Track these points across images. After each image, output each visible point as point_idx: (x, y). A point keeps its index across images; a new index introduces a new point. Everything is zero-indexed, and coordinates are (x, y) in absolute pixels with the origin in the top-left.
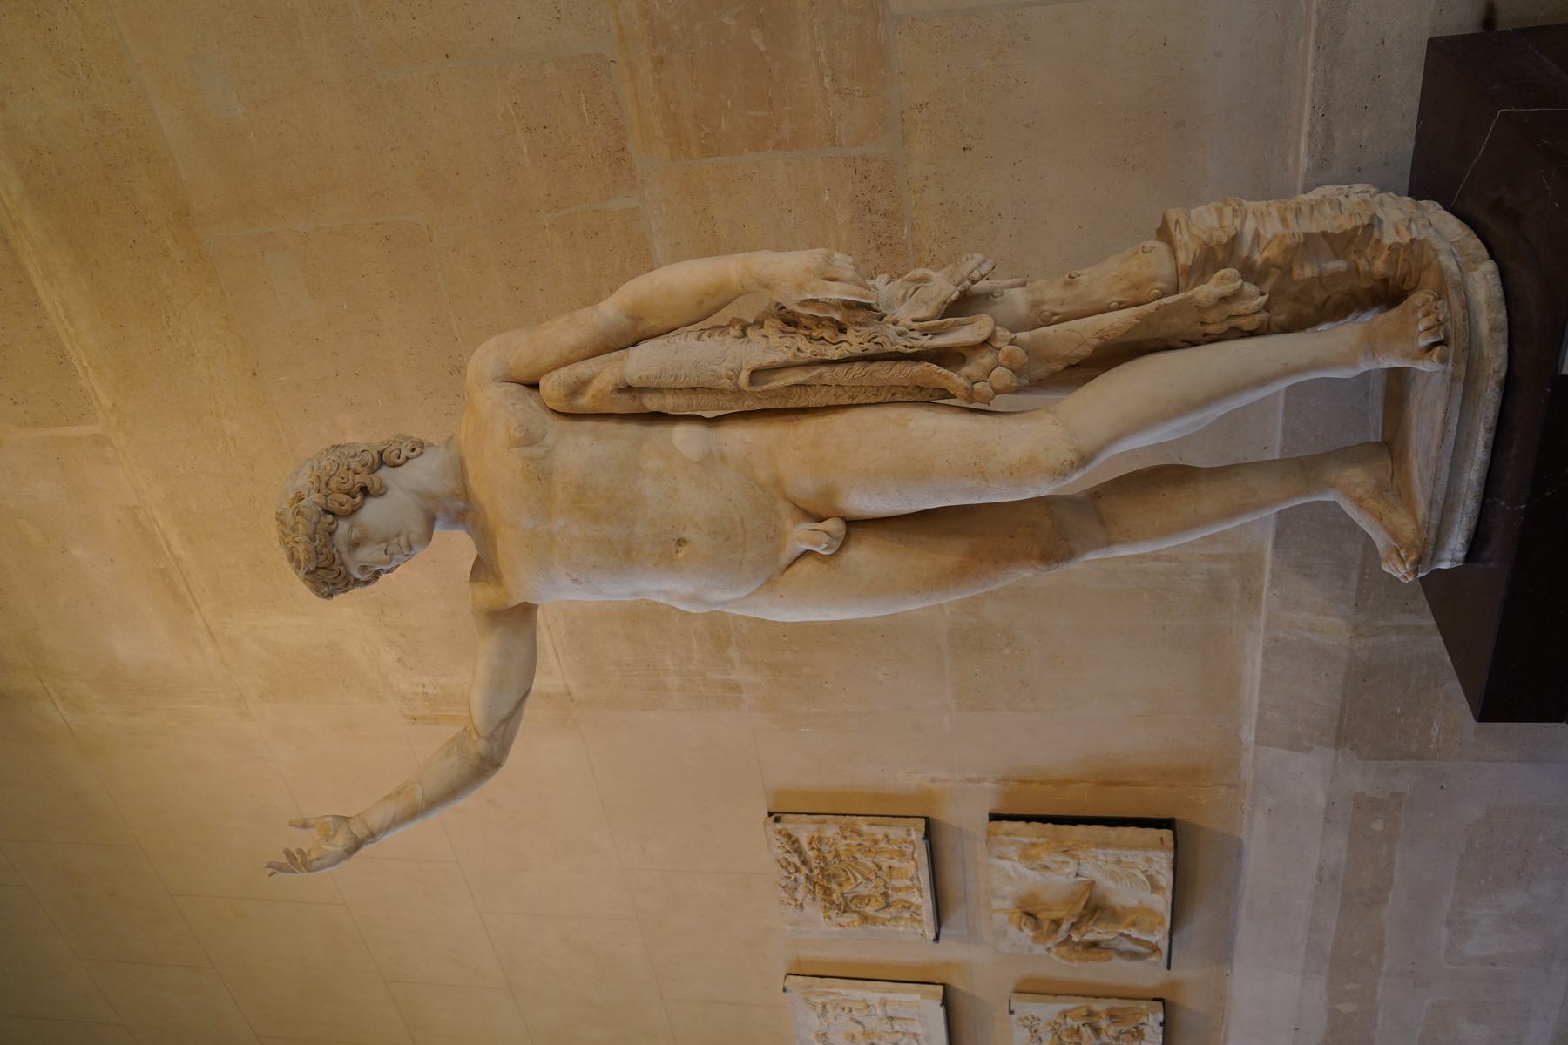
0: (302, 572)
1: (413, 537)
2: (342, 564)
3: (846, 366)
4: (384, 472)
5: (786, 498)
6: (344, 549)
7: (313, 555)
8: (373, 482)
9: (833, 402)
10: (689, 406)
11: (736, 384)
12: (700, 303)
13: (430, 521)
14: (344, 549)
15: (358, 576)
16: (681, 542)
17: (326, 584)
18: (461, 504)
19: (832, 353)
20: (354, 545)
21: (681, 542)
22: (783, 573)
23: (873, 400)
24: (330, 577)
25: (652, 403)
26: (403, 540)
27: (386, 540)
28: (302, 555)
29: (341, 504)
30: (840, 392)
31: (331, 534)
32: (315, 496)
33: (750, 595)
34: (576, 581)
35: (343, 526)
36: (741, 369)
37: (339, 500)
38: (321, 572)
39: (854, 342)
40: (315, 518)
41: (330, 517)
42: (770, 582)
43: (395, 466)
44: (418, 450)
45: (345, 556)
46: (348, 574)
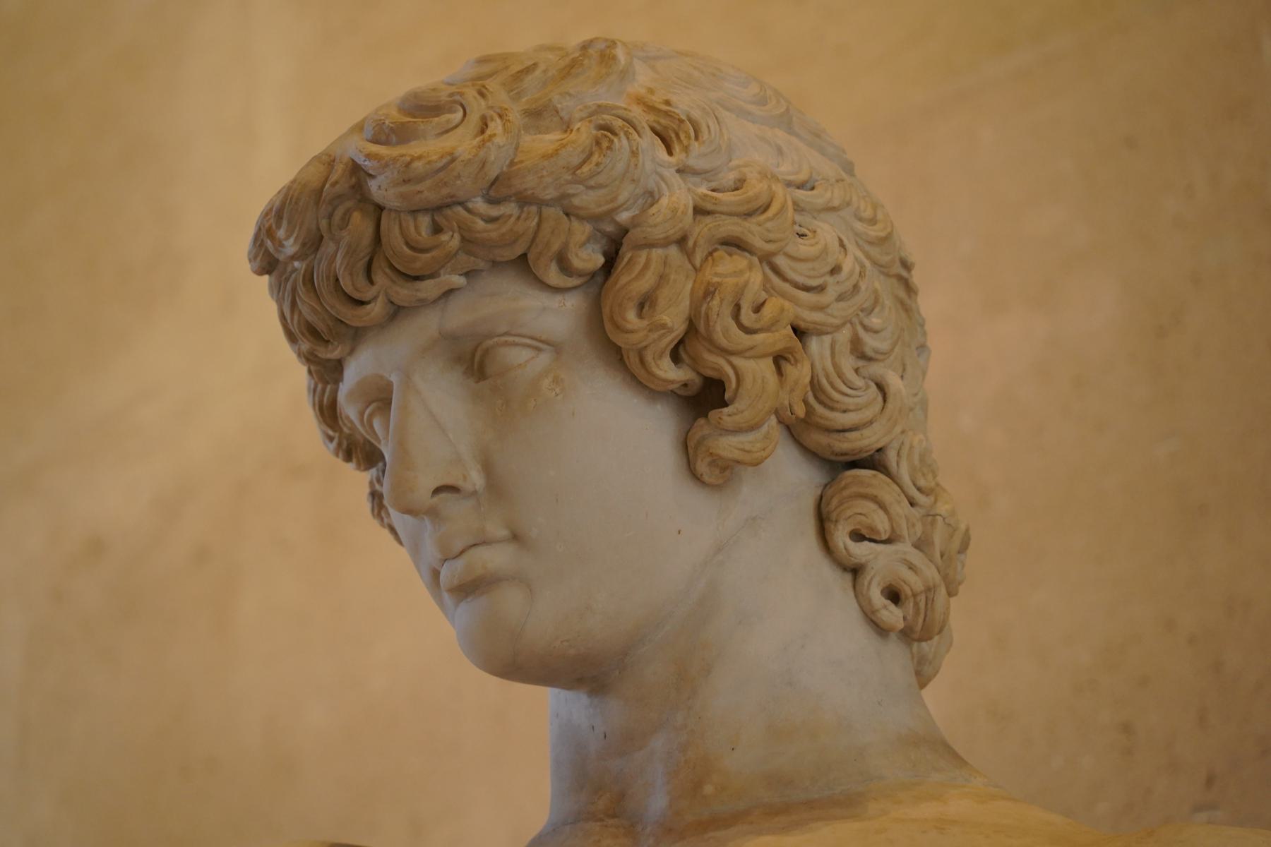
0: (358, 149)
1: (511, 601)
2: (397, 312)
4: (790, 478)
6: (458, 316)
7: (428, 193)
8: (745, 428)
13: (585, 671)
14: (458, 316)
15: (354, 372)
17: (313, 244)
18: (657, 803)
20: (475, 360)
24: (338, 259)
26: (496, 558)
27: (496, 488)
28: (428, 147)
29: (645, 304)
31: (523, 265)
32: (678, 196)
35: (556, 314)
37: (666, 293)
38: (360, 225)
40: (586, 199)
41: (590, 258)
44: (892, 615)
45: (428, 324)
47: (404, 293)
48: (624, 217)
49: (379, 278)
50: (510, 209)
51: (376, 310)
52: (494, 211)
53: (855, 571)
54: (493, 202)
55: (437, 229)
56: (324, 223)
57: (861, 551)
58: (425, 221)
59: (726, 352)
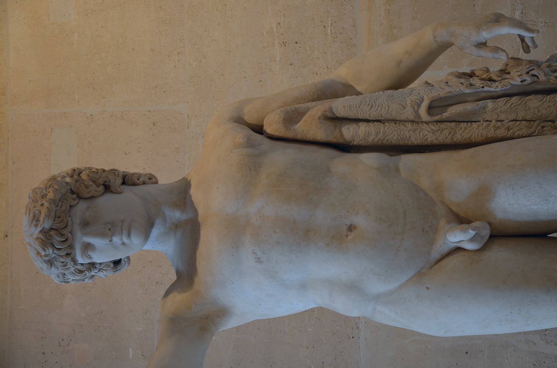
3: (506, 99)
5: (443, 203)
6: (77, 220)
7: (53, 214)
9: (491, 133)
10: (377, 134)
11: (417, 112)
12: (400, 62)
14: (77, 220)
16: (351, 228)
17: (53, 246)
19: (496, 88)
21: (351, 228)
22: (431, 267)
23: (524, 131)
25: (349, 133)
30: (499, 124)
33: (401, 287)
34: (259, 260)
35: (82, 206)
36: (422, 100)
39: (516, 79)
42: (420, 275)
43: (134, 184)
44: (154, 180)
46: (71, 247)
47: (69, 229)
48: (69, 188)
49: (64, 232)
50: (60, 204)
51: (70, 235)
52: (60, 205)
53: (144, 183)
54: (57, 206)
55: (59, 217)
56: (50, 241)
57: (141, 179)
58: (57, 219)
59: (100, 177)
